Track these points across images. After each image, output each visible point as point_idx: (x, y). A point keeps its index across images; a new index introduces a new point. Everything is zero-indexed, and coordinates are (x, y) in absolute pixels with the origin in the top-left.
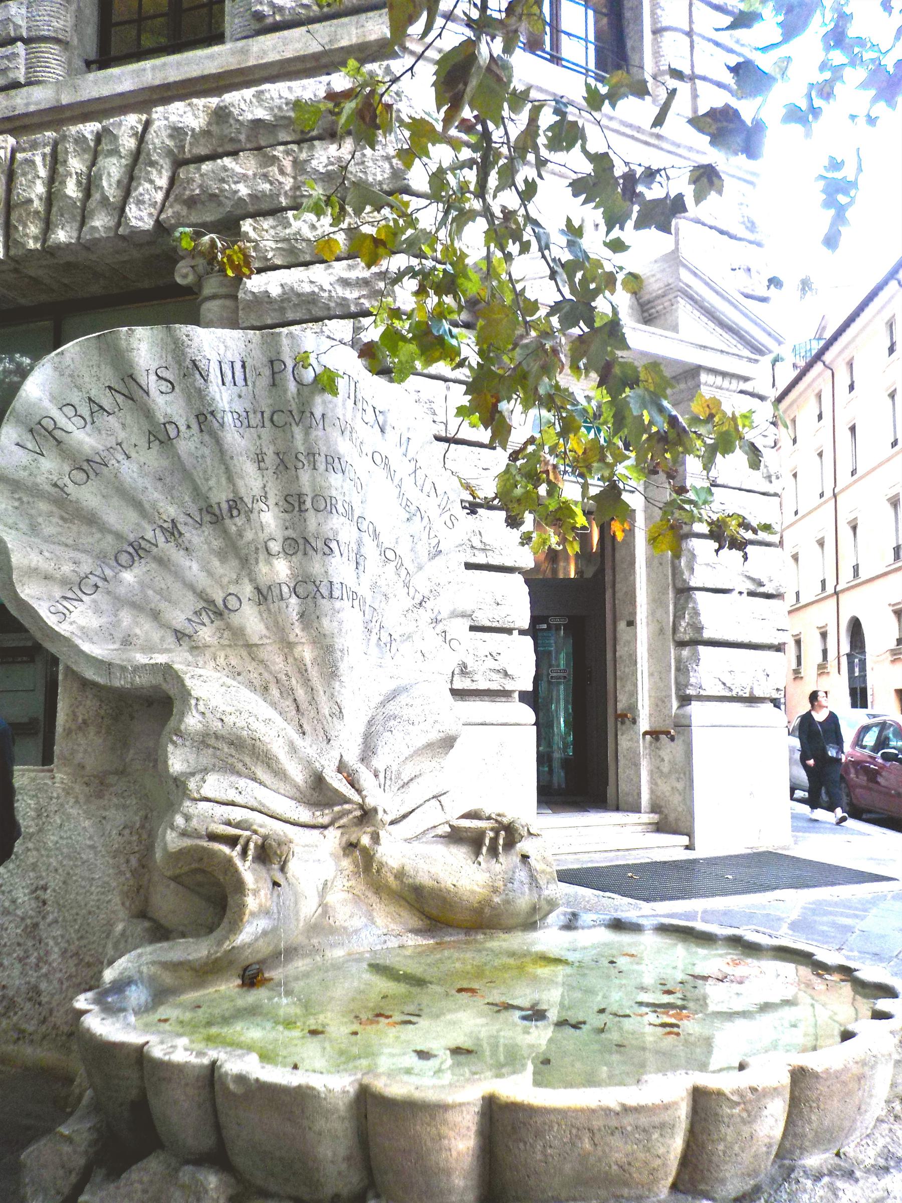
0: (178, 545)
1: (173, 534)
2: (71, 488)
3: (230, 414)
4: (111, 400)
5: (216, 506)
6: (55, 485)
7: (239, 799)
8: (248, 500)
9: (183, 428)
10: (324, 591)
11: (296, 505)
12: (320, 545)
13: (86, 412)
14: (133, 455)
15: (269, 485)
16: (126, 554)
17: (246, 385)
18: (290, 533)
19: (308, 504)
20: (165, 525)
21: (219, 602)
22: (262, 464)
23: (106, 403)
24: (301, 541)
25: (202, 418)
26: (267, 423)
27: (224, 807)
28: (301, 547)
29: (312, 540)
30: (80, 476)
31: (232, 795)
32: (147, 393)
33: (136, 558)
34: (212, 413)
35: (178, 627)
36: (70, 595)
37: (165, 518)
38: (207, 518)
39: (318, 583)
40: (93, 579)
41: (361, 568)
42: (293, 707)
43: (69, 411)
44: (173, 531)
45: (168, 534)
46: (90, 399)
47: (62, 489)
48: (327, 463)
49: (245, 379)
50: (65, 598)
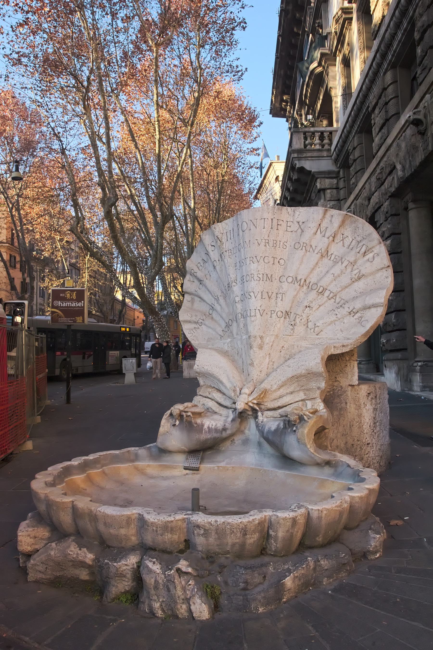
7: (210, 396)
10: (249, 315)
13: (202, 264)
14: (211, 275)
19: (245, 280)
27: (204, 399)
31: (207, 394)
35: (220, 333)
36: (196, 327)
40: (201, 321)
41: (279, 299)
44: (217, 300)
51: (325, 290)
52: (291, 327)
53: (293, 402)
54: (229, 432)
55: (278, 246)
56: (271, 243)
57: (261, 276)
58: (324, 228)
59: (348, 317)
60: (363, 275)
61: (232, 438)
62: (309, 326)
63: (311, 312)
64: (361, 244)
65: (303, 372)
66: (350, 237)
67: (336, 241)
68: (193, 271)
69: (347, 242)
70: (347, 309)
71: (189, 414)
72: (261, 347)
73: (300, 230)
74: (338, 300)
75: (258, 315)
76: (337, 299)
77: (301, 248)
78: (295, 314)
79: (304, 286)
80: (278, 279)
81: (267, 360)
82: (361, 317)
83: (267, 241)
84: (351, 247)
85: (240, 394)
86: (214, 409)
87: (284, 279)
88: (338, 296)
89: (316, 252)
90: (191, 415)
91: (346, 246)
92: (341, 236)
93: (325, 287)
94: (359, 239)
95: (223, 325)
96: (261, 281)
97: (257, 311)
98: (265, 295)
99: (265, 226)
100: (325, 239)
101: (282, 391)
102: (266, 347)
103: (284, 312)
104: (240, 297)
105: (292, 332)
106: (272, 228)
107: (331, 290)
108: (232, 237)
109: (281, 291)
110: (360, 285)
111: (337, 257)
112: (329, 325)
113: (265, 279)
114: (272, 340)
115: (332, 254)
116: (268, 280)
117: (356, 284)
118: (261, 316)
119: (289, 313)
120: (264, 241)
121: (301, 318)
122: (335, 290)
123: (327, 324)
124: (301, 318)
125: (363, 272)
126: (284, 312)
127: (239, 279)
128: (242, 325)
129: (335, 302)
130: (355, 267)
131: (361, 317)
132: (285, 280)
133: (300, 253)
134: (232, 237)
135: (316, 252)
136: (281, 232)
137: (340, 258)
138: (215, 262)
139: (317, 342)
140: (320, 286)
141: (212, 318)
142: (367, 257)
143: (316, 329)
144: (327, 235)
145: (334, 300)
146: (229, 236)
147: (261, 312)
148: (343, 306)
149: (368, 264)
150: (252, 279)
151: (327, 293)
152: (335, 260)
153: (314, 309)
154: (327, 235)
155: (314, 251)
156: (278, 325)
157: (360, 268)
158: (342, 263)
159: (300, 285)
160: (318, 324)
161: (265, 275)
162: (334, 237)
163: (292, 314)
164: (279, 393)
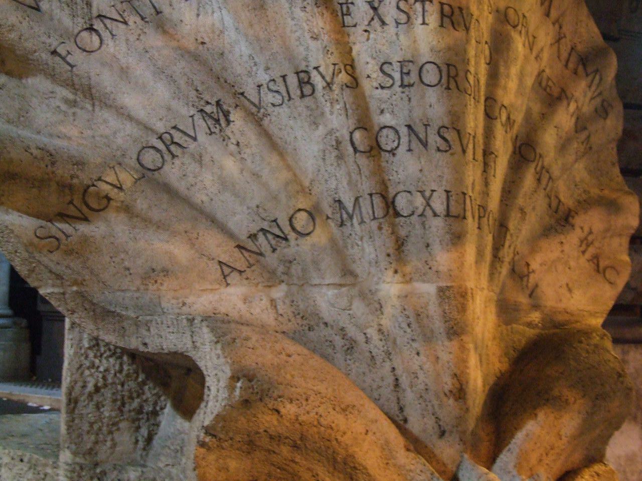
1: (217, 121)
2: (77, 57)
6: (54, 53)
11: (397, 76)
16: (152, 151)
20: (208, 109)
24: (404, 131)
28: (404, 140)
33: (168, 157)
35: (224, 258)
39: (427, 194)
45: (210, 122)
47: (64, 59)
111: (550, 83)
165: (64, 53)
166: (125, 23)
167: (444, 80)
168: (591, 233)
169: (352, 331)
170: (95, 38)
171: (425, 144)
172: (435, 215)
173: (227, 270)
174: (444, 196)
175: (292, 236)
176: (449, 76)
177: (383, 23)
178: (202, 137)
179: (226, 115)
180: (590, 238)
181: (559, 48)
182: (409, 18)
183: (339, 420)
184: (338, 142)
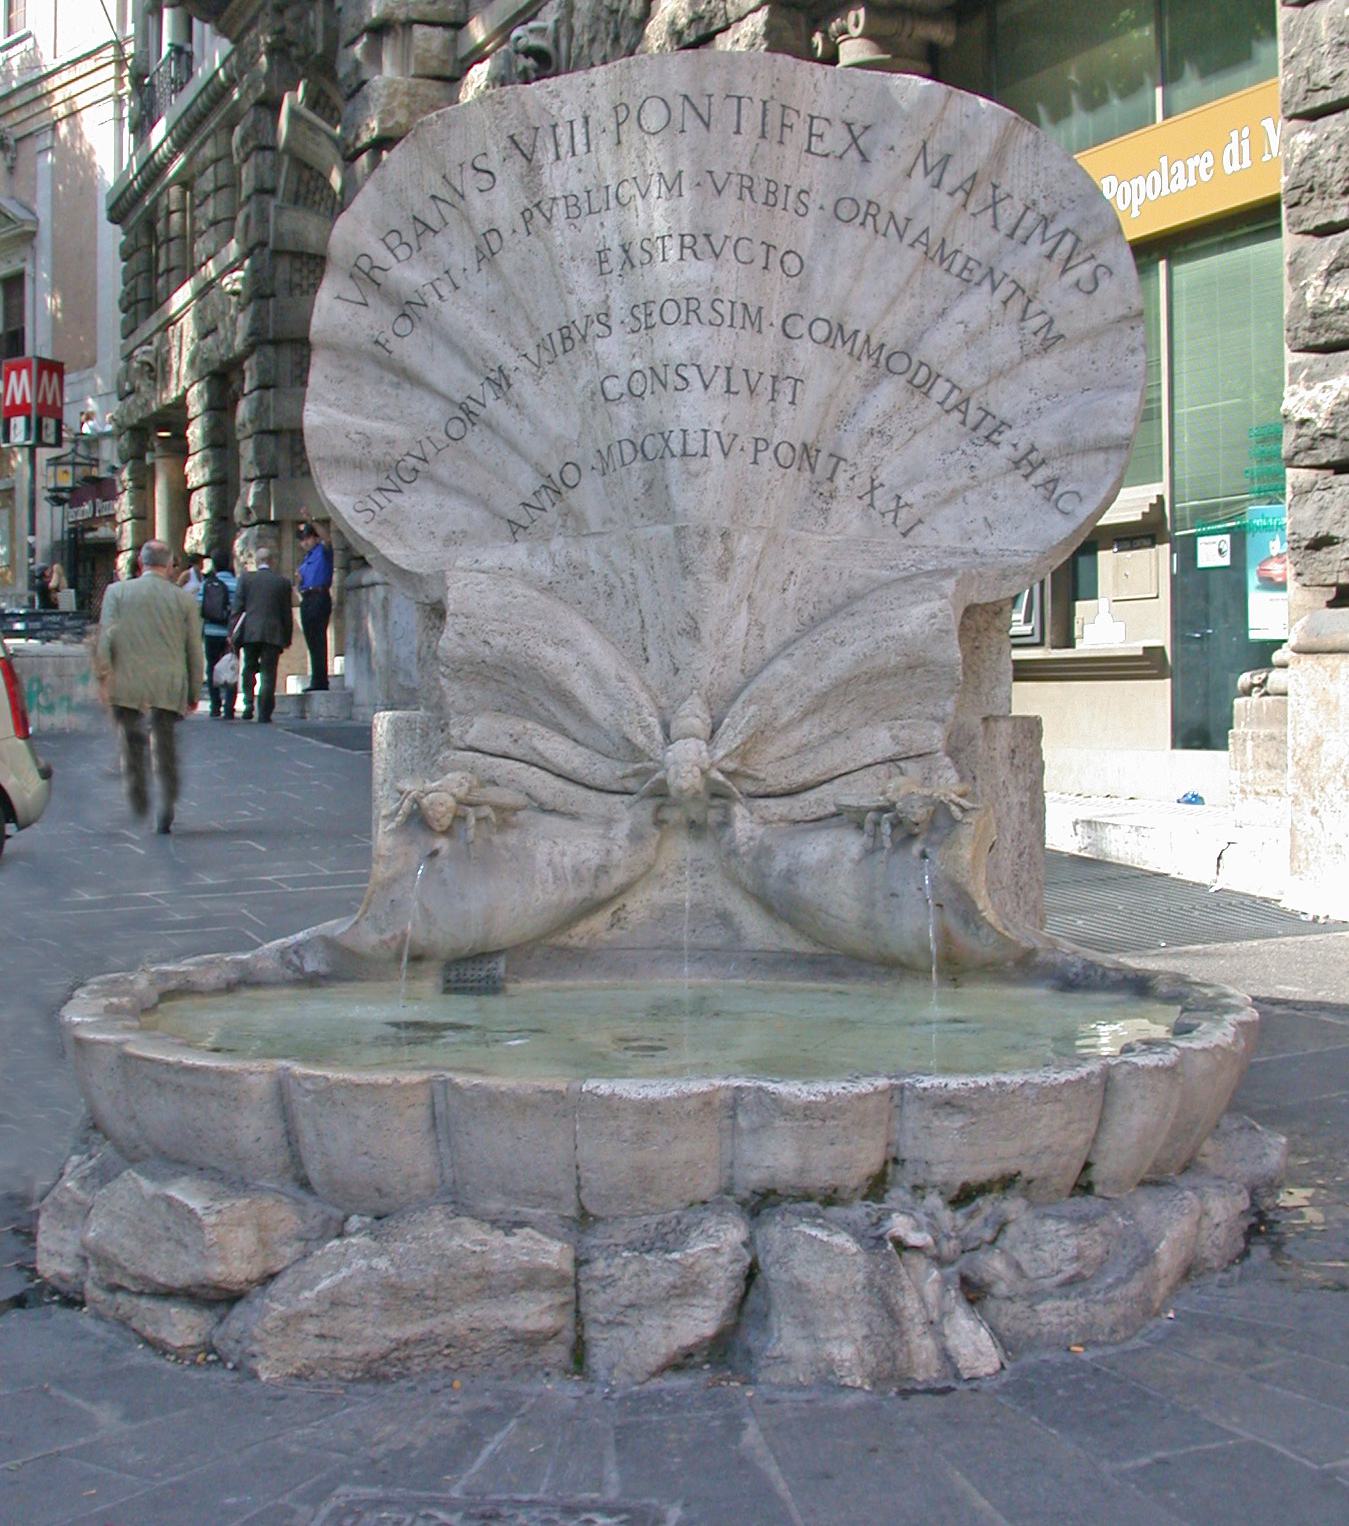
0: (508, 401)
2: (394, 344)
3: (562, 202)
4: (436, 214)
5: (547, 339)
6: (377, 342)
7: (514, 751)
8: (580, 324)
9: (506, 235)
10: (676, 447)
12: (672, 378)
15: (612, 295)
16: (457, 422)
17: (589, 151)
18: (637, 364)
19: (656, 318)
20: (492, 376)
21: (556, 477)
22: (605, 265)
23: (433, 220)
24: (648, 373)
25: (527, 214)
26: (613, 203)
29: (660, 370)
30: (404, 325)
31: (505, 744)
32: (462, 196)
33: (469, 425)
34: (537, 205)
37: (491, 365)
38: (546, 357)
41: (785, 398)
42: (637, 623)
43: (393, 240)
46: (415, 218)
48: (682, 246)
49: (588, 144)
50: (380, 489)
51: (933, 377)
52: (820, 504)
53: (852, 766)
54: (619, 878)
55: (780, 205)
56: (760, 189)
57: (724, 308)
58: (937, 158)
59: (1010, 479)
60: (1062, 336)
61: (619, 902)
62: (877, 504)
63: (885, 452)
64: (1053, 229)
65: (894, 660)
66: (1016, 198)
67: (972, 207)
68: (364, 263)
69: (1008, 214)
70: (1006, 450)
71: (487, 811)
72: (723, 571)
73: (853, 154)
74: (974, 415)
75: (716, 456)
76: (970, 411)
77: (860, 219)
78: (831, 455)
79: (864, 358)
80: (778, 322)
81: (742, 620)
82: (1055, 481)
83: (747, 182)
84: (1020, 233)
85: (667, 736)
86: (545, 795)
87: (801, 327)
88: (973, 404)
89: (907, 240)
90: (493, 816)
91: (1004, 228)
92: (990, 192)
93: (936, 368)
94: (1044, 208)
95: (528, 481)
96: (725, 328)
97: (712, 437)
98: (739, 383)
99: (743, 123)
100: (941, 197)
101: (807, 731)
102: (739, 572)
103: (798, 446)
104: (623, 381)
105: (821, 520)
106: (763, 136)
107: (955, 379)
108: (580, 148)
109: (789, 371)
110: (1044, 369)
111: (971, 264)
112: (947, 501)
113: (738, 321)
114: (758, 548)
115: (957, 252)
116: (748, 324)
117: (1033, 364)
118: (726, 455)
119: (814, 453)
120: (735, 179)
121: (851, 471)
122: (970, 380)
123: (938, 499)
124: (851, 471)
125: (1059, 327)
126: (798, 446)
127: (619, 311)
128: (636, 486)
129: (963, 423)
130: (1034, 308)
131: (1055, 481)
132: (805, 332)
133: (851, 238)
134: (580, 148)
135: (907, 240)
136: (791, 153)
137: (984, 270)
138: (493, 238)
139: (907, 559)
140: (922, 364)
141: (468, 455)
142: (1071, 277)
143: (903, 514)
144: (950, 180)
145: (960, 416)
146: (565, 140)
147: (726, 441)
148: (995, 437)
149: (1076, 300)
150: (693, 318)
151: (940, 389)
152: (965, 275)
153: (896, 444)
154: (950, 180)
155: (901, 237)
156: (780, 494)
157: (1052, 310)
158: (994, 288)
159: (851, 354)
160: (907, 497)
161: (739, 307)
162: (968, 194)
163: (823, 456)
164: (797, 736)
165: (383, 341)
166: (425, 305)
167: (683, 316)
168: (1033, 449)
169: (613, 579)
170: (408, 322)
171: (665, 386)
172: (673, 456)
173: (515, 527)
174: (681, 435)
175: (564, 489)
176: (688, 311)
177: (633, 266)
178: (490, 401)
179: (507, 378)
180: (1033, 457)
181: (995, 215)
182: (651, 256)
183: (550, 652)
184: (593, 393)
